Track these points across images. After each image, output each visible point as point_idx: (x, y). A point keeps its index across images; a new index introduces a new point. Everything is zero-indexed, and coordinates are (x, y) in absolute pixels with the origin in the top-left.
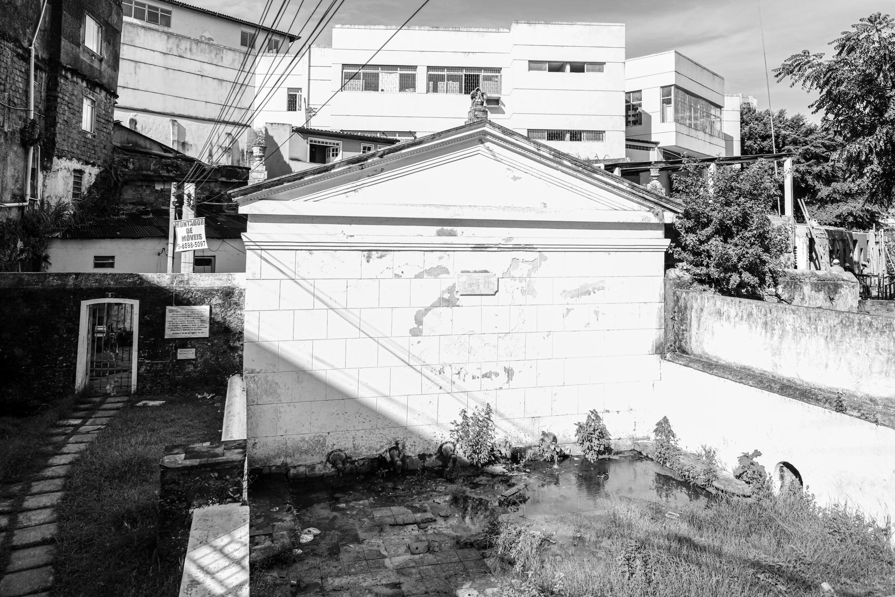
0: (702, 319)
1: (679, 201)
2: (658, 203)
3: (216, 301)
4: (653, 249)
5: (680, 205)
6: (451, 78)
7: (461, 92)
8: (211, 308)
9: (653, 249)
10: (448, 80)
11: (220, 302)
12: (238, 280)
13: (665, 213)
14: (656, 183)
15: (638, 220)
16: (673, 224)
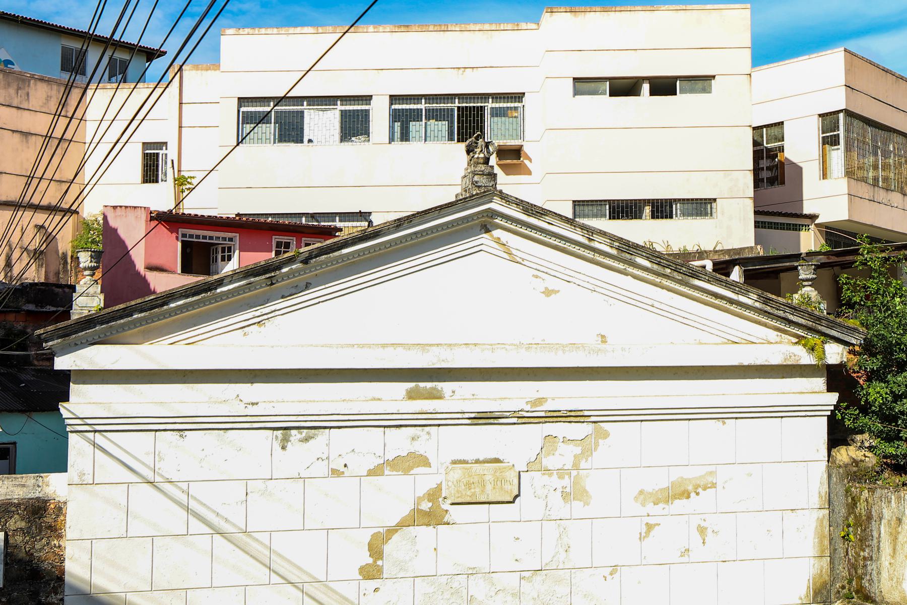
0: (900, 537)
1: (851, 323)
2: (814, 328)
3: (16, 523)
4: (807, 412)
5: (855, 330)
6: (433, 115)
7: (451, 138)
8: (6, 535)
9: (807, 412)
10: (428, 118)
11: (22, 524)
12: (54, 485)
13: (827, 346)
14: (809, 291)
15: (776, 360)
16: (841, 366)
